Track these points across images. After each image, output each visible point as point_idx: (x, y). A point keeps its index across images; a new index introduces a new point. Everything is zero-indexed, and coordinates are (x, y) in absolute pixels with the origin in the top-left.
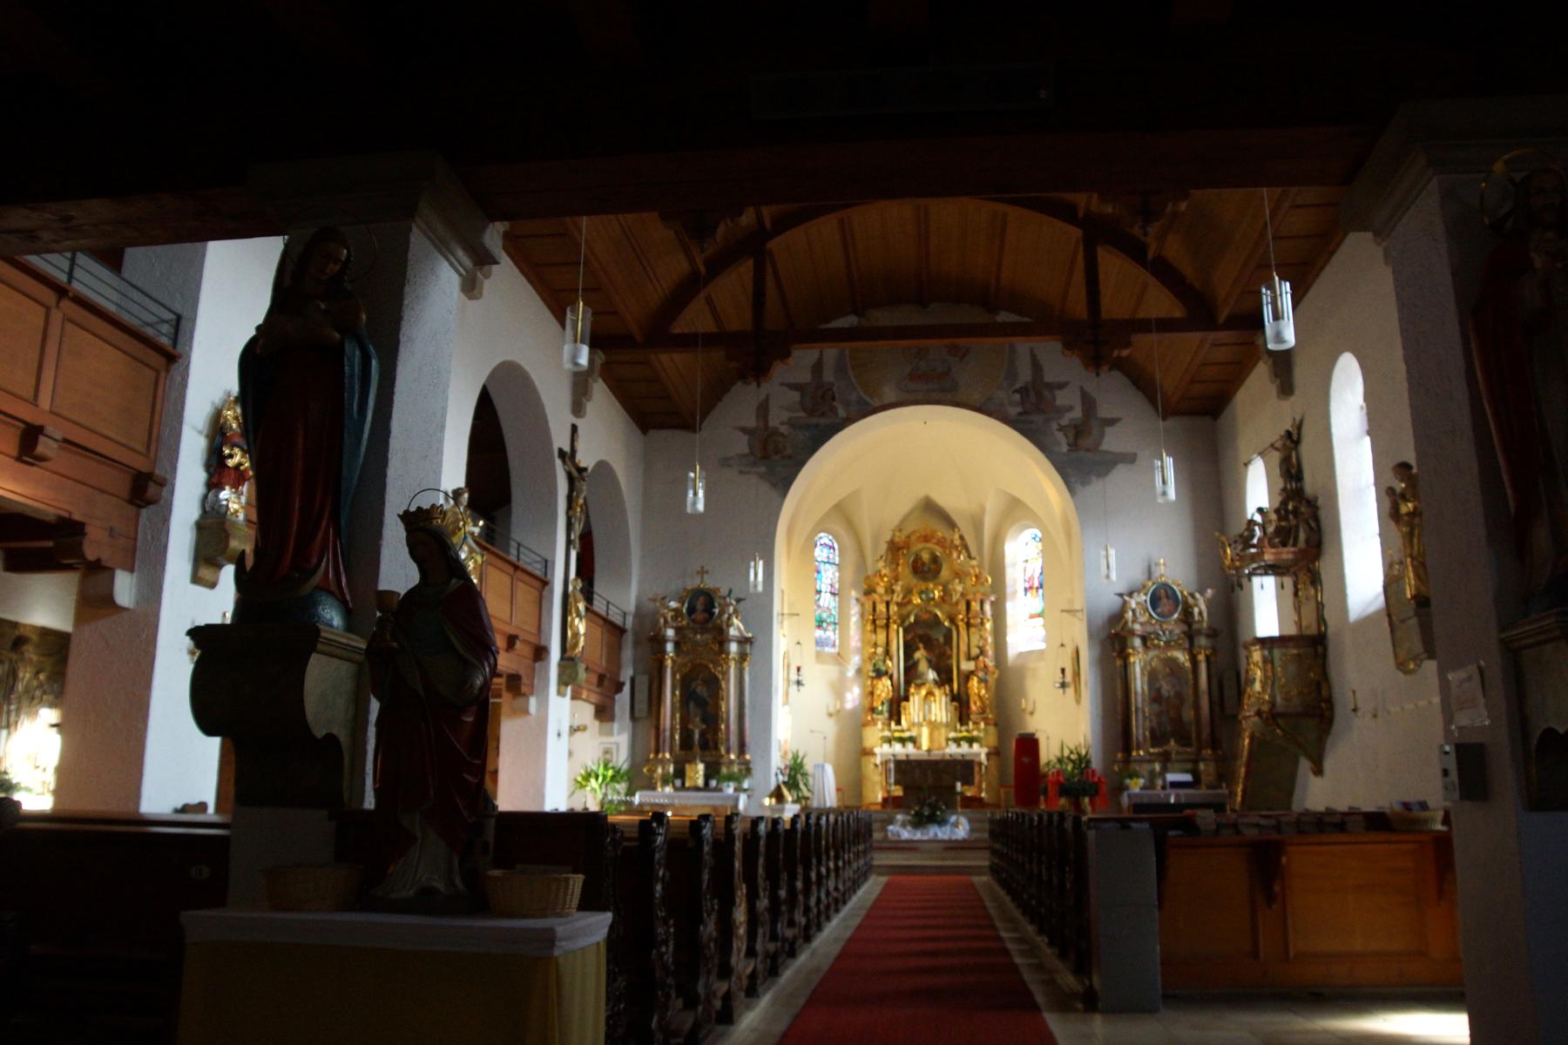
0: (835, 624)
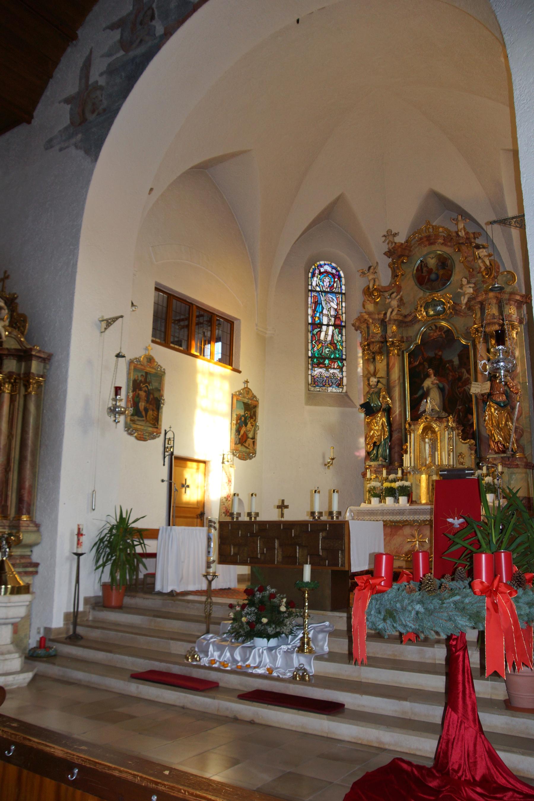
0: (342, 360)
